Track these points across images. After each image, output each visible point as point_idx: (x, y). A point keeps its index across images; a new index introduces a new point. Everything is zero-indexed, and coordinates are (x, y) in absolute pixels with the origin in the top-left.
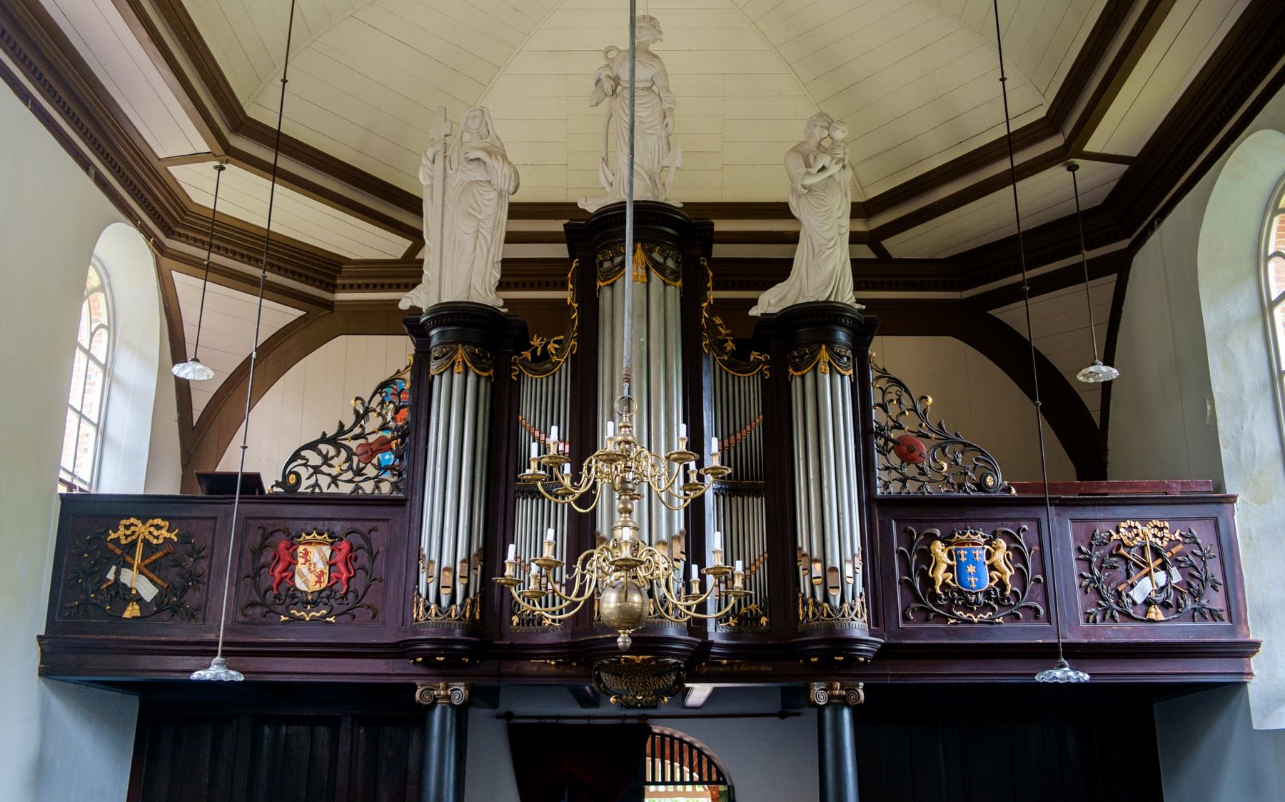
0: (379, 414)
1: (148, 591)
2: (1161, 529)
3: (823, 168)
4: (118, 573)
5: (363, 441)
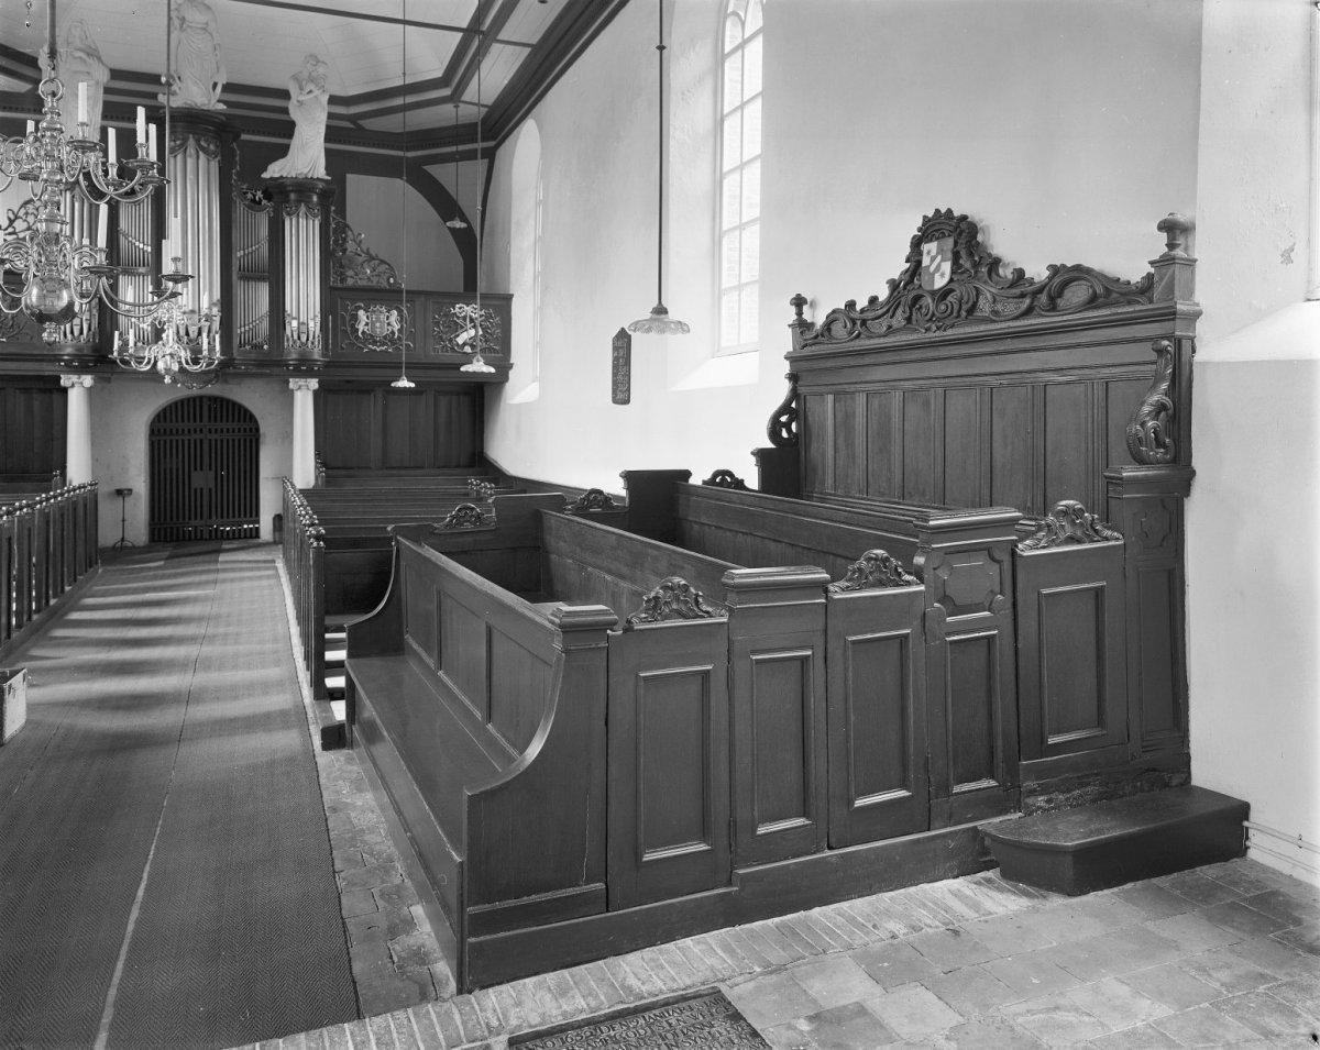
0: (25, 220)
3: (311, 92)
5: (15, 236)
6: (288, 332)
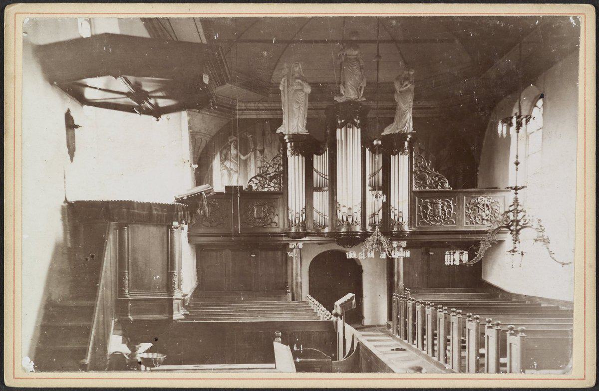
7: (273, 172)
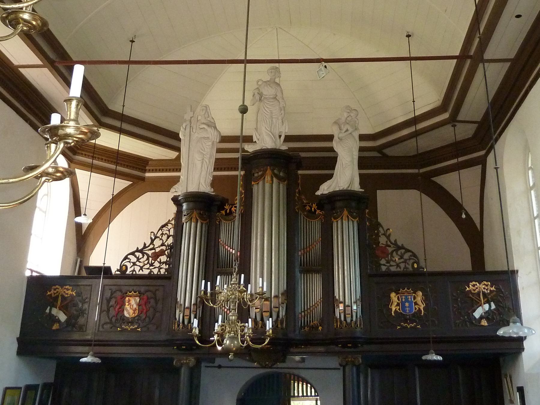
0: (161, 239)
1: (63, 317)
2: (487, 285)
4: (50, 310)
5: (153, 251)
6: (337, 315)
7: (159, 247)
